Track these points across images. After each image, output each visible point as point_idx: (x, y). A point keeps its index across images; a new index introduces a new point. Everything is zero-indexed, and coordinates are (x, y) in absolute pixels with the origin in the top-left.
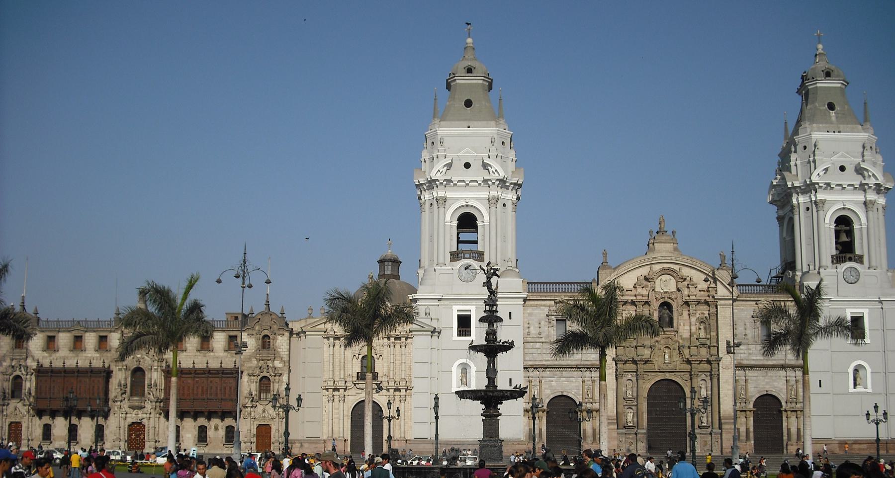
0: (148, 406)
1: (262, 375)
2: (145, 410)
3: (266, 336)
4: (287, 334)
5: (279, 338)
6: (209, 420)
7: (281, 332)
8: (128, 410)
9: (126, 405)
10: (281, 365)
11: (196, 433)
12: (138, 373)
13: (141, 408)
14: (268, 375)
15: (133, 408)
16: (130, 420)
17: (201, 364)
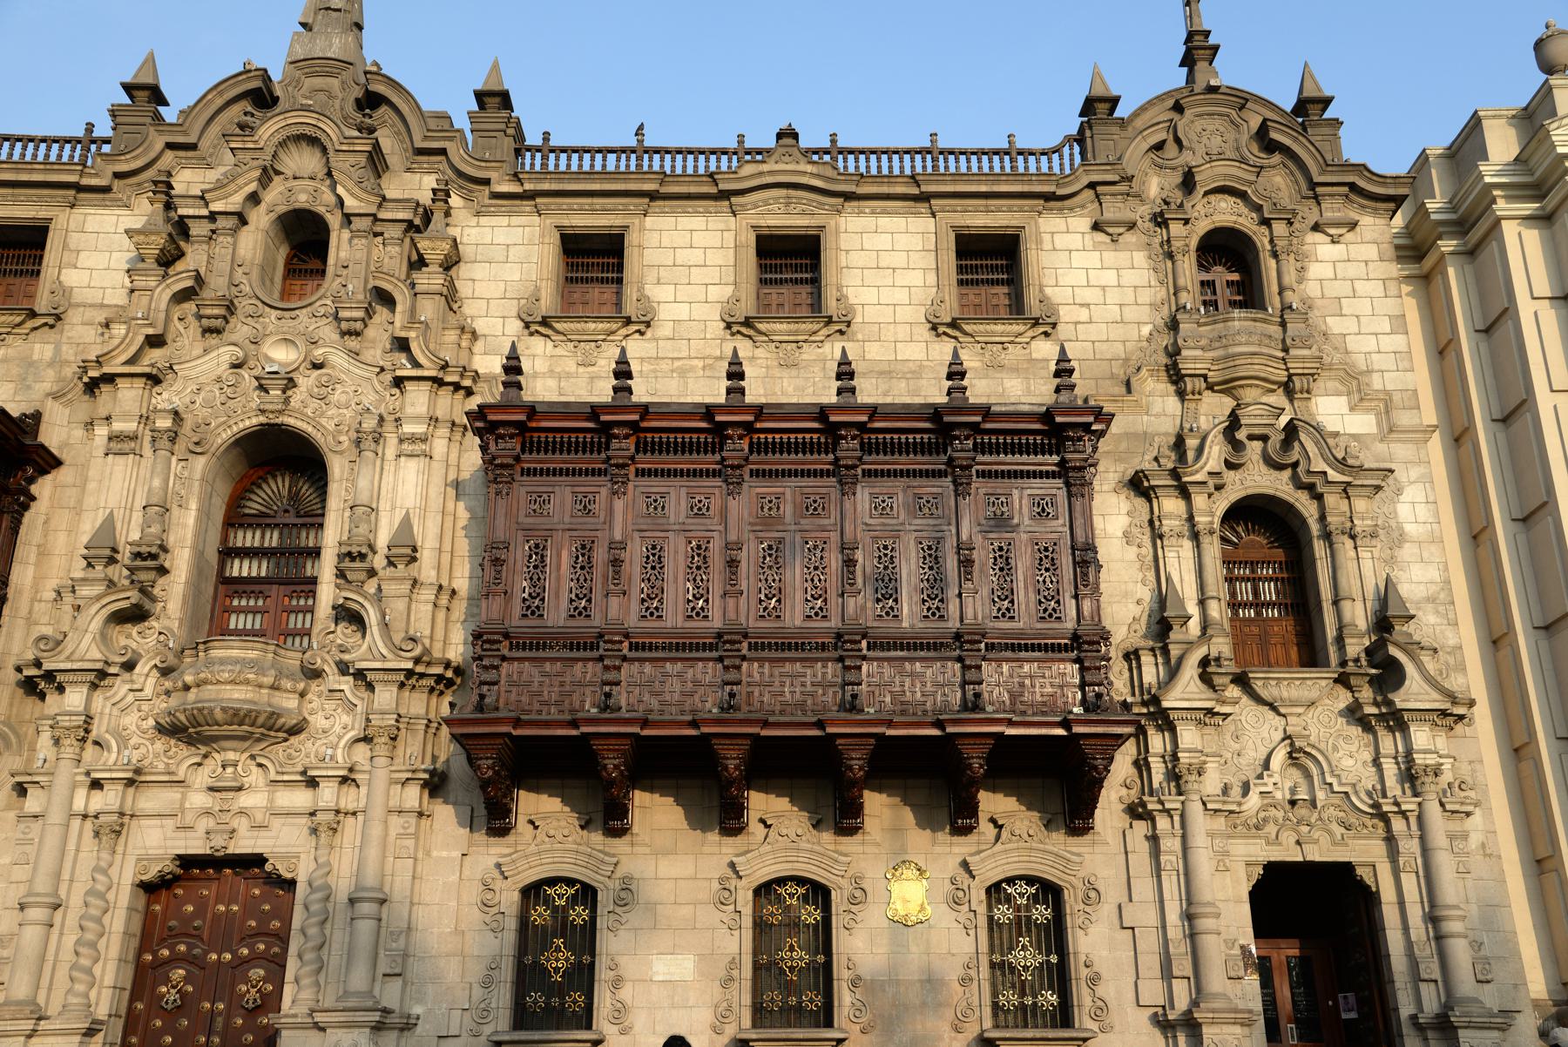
0: (332, 723)
1: (1239, 486)
2: (305, 751)
3: (1226, 250)
4: (1377, 232)
5: (1322, 249)
6: (843, 817)
7: (1333, 209)
8: (157, 753)
9: (129, 714)
10: (1362, 424)
11: (738, 943)
12: (279, 463)
13: (267, 729)
14: (1278, 485)
15: (186, 730)
16: (157, 842)
17: (791, 378)
